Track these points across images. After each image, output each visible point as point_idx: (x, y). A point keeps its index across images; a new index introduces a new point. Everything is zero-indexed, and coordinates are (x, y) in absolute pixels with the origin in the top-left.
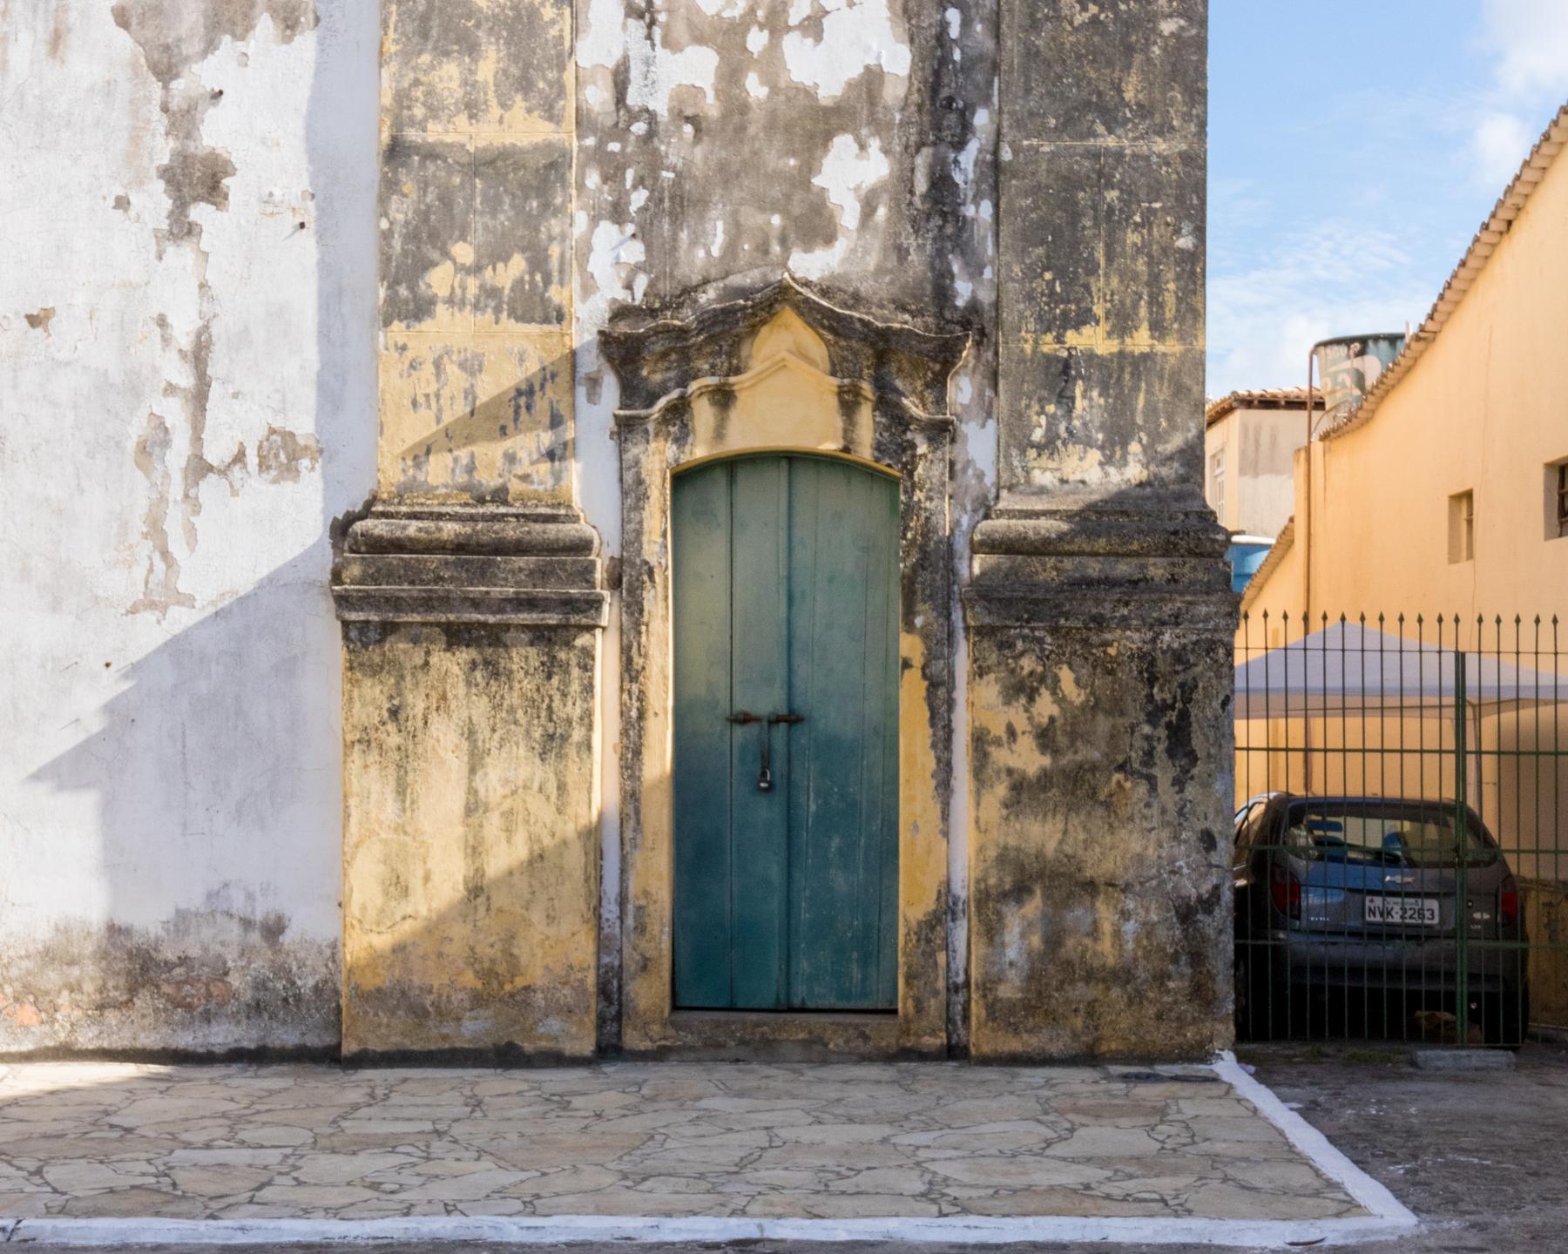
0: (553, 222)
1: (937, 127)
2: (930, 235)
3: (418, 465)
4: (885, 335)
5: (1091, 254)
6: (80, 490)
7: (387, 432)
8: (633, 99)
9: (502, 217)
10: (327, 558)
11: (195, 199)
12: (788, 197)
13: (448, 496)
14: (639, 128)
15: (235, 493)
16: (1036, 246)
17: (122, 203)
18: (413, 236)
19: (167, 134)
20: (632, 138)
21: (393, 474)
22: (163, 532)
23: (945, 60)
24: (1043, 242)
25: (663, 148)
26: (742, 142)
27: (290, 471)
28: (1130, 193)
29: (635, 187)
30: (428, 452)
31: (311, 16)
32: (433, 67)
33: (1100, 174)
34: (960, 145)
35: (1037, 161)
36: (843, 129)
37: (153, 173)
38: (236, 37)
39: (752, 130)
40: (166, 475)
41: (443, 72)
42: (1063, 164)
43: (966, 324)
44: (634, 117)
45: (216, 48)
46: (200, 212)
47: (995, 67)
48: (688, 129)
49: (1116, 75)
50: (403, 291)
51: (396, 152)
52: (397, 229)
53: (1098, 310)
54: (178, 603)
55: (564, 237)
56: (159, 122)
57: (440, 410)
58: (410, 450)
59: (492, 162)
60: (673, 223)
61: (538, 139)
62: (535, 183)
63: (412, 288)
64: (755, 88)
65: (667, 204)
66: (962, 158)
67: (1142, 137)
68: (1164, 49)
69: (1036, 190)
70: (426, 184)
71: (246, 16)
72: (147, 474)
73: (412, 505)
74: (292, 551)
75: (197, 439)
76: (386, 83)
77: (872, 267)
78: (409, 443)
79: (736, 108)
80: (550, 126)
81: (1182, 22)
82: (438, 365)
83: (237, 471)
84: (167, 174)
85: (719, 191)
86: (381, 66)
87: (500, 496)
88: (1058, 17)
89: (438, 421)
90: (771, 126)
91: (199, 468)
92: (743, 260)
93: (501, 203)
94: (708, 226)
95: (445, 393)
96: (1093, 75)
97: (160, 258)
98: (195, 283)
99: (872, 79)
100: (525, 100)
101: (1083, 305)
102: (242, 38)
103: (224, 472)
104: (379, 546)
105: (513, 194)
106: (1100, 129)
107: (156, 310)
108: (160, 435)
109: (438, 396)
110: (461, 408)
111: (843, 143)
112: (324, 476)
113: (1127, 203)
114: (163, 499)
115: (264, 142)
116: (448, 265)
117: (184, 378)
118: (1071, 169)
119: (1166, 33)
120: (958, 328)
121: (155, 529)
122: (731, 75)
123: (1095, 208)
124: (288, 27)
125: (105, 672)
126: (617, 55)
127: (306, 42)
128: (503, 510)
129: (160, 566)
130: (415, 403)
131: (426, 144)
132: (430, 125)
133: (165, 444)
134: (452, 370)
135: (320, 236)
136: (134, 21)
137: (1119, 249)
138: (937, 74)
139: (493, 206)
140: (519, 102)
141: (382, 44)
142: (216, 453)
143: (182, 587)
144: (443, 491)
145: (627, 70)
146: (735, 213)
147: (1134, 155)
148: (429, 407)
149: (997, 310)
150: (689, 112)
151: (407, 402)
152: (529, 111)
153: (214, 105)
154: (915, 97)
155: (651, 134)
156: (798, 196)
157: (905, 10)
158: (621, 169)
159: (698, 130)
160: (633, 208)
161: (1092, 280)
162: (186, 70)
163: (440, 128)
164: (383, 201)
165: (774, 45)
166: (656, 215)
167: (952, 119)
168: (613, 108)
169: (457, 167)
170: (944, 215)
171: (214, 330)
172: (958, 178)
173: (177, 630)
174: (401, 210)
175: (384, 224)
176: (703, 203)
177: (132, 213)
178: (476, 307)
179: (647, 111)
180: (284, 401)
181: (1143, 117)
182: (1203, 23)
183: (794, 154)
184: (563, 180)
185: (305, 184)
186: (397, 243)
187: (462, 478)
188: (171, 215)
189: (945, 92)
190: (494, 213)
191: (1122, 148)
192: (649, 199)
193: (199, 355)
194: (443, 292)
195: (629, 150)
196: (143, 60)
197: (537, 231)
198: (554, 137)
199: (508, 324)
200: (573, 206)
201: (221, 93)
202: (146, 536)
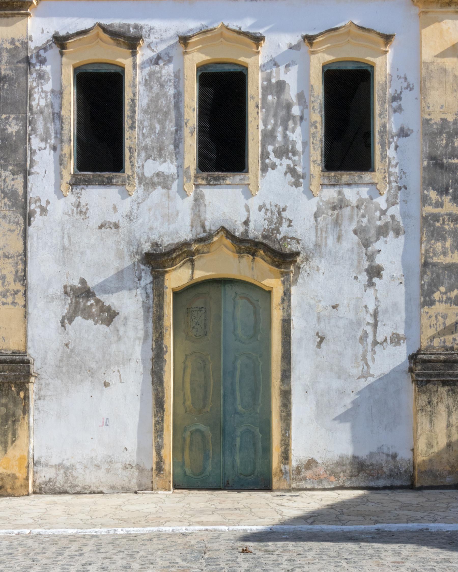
3: (431, 341)
6: (345, 348)
7: (424, 333)
10: (407, 365)
11: (374, 277)
13: (439, 349)
15: (384, 349)
17: (356, 278)
18: (430, 285)
19: (367, 261)
21: (425, 344)
22: (367, 359)
27: (398, 343)
30: (434, 338)
31: (403, 231)
37: (363, 270)
38: (384, 237)
40: (367, 345)
41: (437, 245)
45: (379, 239)
46: (375, 280)
50: (427, 299)
51: (426, 265)
52: (426, 283)
54: (370, 376)
56: (365, 258)
57: (437, 328)
58: (429, 338)
63: (430, 298)
72: (362, 345)
73: (430, 351)
74: (399, 363)
75: (375, 336)
78: (429, 336)
82: (436, 317)
83: (385, 344)
84: (367, 270)
87: (452, 348)
89: (436, 330)
91: (375, 343)
95: (438, 324)
97: (365, 291)
98: (374, 297)
102: (386, 237)
103: (382, 344)
104: (424, 361)
107: (364, 304)
108: (365, 335)
109: (436, 324)
110: (442, 327)
112: (407, 344)
114: (366, 351)
115: (391, 262)
116: (439, 292)
117: (371, 321)
121: (364, 358)
125: (352, 394)
127: (402, 238)
128: (453, 352)
129: (365, 367)
130: (430, 326)
131: (433, 262)
133: (367, 337)
134: (440, 318)
135: (406, 285)
136: (358, 233)
139: (450, 277)
142: (380, 339)
143: (371, 372)
144: (438, 348)
148: (434, 327)
151: (428, 326)
153: (379, 253)
162: (371, 245)
164: (422, 278)
171: (379, 309)
173: (370, 383)
174: (427, 279)
175: (423, 282)
177: (358, 280)
178: (446, 302)
180: (396, 326)
185: (401, 273)
186: (426, 287)
187: (442, 344)
188: (368, 281)
193: (375, 315)
194: (437, 299)
199: (454, 306)
201: (380, 250)
202: (362, 360)
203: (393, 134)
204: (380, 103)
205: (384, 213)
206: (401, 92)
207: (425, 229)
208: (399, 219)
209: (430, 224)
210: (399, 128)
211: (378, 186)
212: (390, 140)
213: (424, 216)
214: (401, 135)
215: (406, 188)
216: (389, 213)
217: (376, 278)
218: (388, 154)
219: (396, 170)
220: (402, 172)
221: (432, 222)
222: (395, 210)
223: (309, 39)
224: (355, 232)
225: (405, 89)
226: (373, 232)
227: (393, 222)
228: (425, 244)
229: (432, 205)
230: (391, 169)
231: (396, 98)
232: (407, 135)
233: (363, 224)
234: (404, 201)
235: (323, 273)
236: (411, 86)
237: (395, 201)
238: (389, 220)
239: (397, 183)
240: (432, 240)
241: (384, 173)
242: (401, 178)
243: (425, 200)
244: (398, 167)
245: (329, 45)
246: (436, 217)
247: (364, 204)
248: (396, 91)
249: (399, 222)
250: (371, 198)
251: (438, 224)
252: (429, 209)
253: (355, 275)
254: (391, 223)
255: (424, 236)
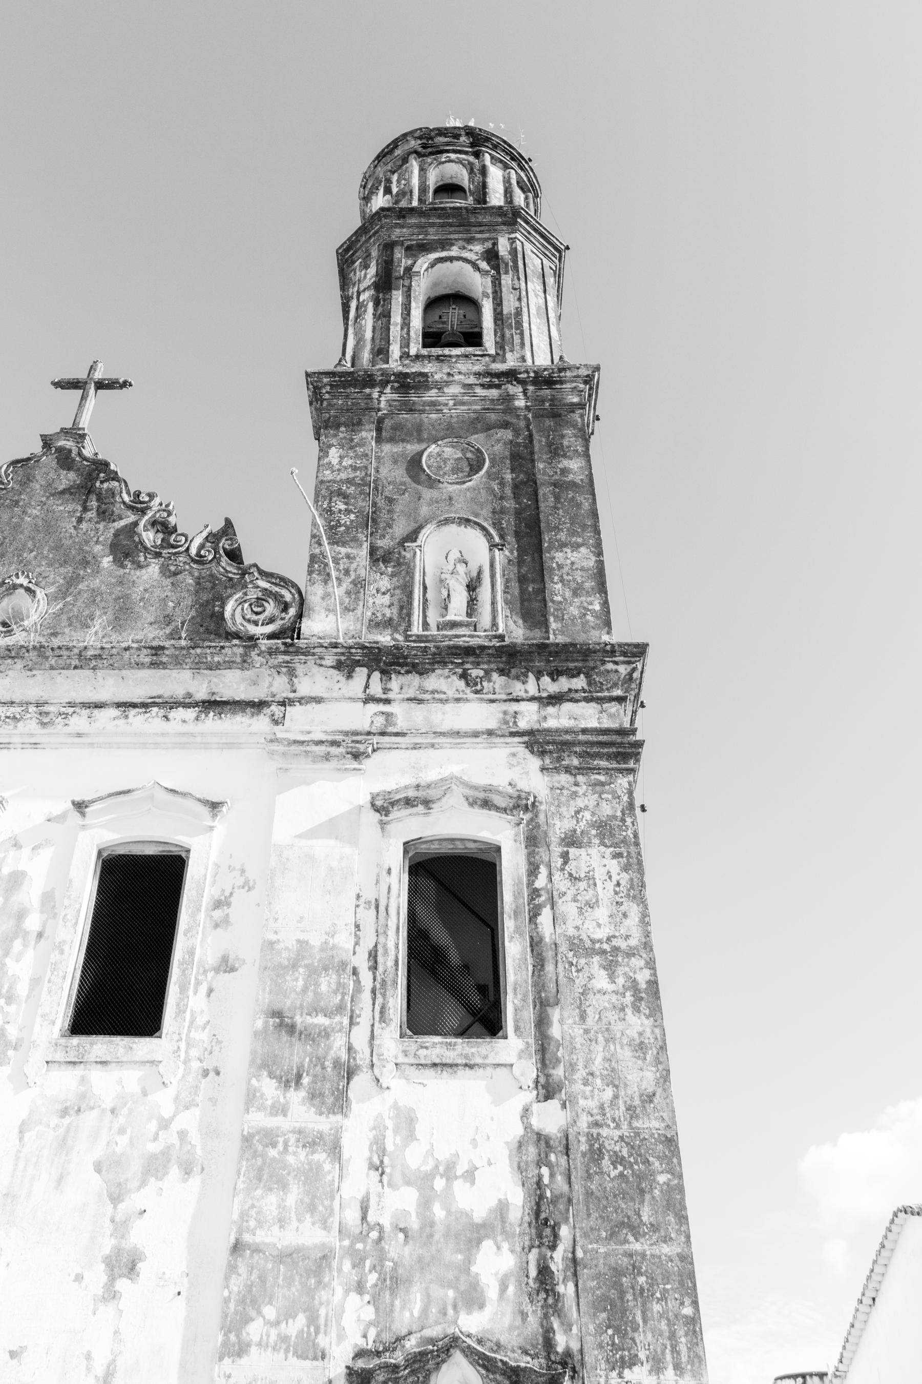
0: (323, 1293)
1: (540, 1236)
2: (540, 1304)
4: (516, 1371)
5: (634, 1318)
8: (371, 1218)
9: (294, 1289)
12: (457, 1279)
14: (374, 1235)
16: (601, 1312)
19: (111, 1235)
20: (370, 1241)
23: (541, 1197)
24: (605, 1310)
25: (387, 1247)
26: (431, 1244)
28: (652, 1279)
29: (370, 1271)
31: (199, 1167)
32: (262, 1197)
33: (634, 1267)
34: (553, 1247)
35: (597, 1258)
36: (487, 1236)
38: (157, 1178)
39: (437, 1237)
42: (612, 1261)
43: (564, 1364)
44: (371, 1229)
47: (570, 1201)
48: (401, 1236)
49: (637, 1206)
53: (642, 1355)
55: (328, 1303)
56: (108, 1227)
59: (291, 1255)
60: (391, 1294)
61: (317, 1241)
62: (314, 1268)
64: (438, 1212)
65: (388, 1282)
66: (555, 1255)
67: (654, 1244)
68: (662, 1191)
69: (598, 1276)
70: (252, 1268)
71: (165, 1166)
76: (235, 1207)
77: (507, 1325)
79: (428, 1224)
80: (324, 1233)
81: (669, 1176)
85: (418, 1274)
86: (234, 1196)
88: (602, 1173)
90: (447, 1235)
92: (432, 1319)
93: (293, 1280)
94: (412, 1296)
96: (624, 1206)
99: (502, 1208)
100: (312, 1217)
101: (632, 1352)
102: (161, 1180)
105: (301, 1275)
106: (631, 1239)
111: (488, 1245)
113: (651, 1285)
118: (617, 1263)
119: (661, 1182)
120: (559, 1367)
122: (425, 1204)
123: (633, 1288)
124: (186, 1173)
126: (363, 1192)
127: (195, 1181)
132: (258, 1232)
136: (104, 1169)
137: (649, 1315)
138: (538, 1204)
140: (308, 1219)
141: (236, 1184)
145: (368, 1200)
146: (427, 1289)
147: (652, 1255)
149: (582, 1355)
150: (402, 1226)
152: (313, 1224)
154: (527, 1219)
155: (380, 1239)
156: (463, 1278)
157: (519, 1167)
158: (363, 1260)
159: (406, 1237)
160: (369, 1285)
161: (636, 1335)
163: (263, 1234)
164: (227, 1278)
165: (449, 1186)
166: (382, 1289)
167: (548, 1231)
168: (360, 1222)
169: (271, 1258)
170: (547, 1291)
172: (553, 1267)
176: (409, 1281)
179: (379, 1224)
181: (654, 1232)
182: (680, 1177)
183: (460, 1251)
184: (330, 1266)
189: (543, 1216)
190: (289, 1286)
191: (645, 1251)
192: (378, 1279)
195: (368, 1248)
196: (105, 1192)
197: (313, 1298)
198: (326, 1240)
200: (335, 1283)
203: (207, 967)
204: (190, 911)
205: (165, 1124)
206: (231, 894)
207: (244, 1163)
208: (195, 1138)
209: (255, 1152)
210: (220, 955)
211: (161, 1068)
212: (200, 978)
213: (245, 1133)
214: (222, 969)
215: (218, 1073)
216: (175, 1127)
217: (124, 1280)
218: (190, 1004)
219: (202, 1036)
220: (215, 1040)
221: (260, 1148)
222: (189, 1120)
223: (80, 806)
224: (98, 1168)
225: (239, 887)
226: (135, 1168)
227: (181, 1145)
228: (241, 1197)
229: (265, 1109)
230: (193, 1034)
231: (218, 904)
232: (233, 969)
233: (118, 1150)
234: (210, 1099)
235: (8, 1265)
236: (251, 884)
237: (193, 1100)
238: (175, 1140)
239: (201, 1061)
240: (256, 1189)
241: (178, 1041)
242: (211, 1053)
243: (251, 1098)
244: (207, 1030)
245: (113, 816)
246: (270, 1138)
247: (128, 1105)
248: (223, 890)
249: (194, 1146)
250: (145, 1093)
251: (272, 1153)
252: (259, 1120)
253: (78, 1270)
254: (177, 1147)
255: (242, 1176)
